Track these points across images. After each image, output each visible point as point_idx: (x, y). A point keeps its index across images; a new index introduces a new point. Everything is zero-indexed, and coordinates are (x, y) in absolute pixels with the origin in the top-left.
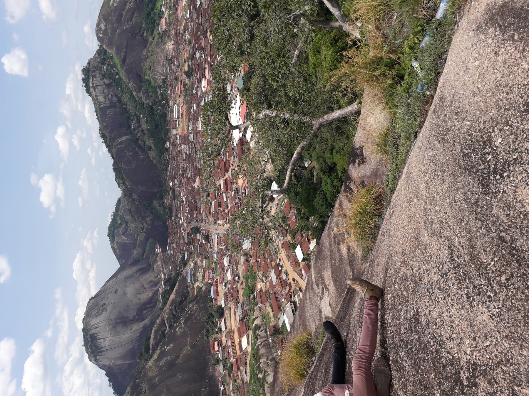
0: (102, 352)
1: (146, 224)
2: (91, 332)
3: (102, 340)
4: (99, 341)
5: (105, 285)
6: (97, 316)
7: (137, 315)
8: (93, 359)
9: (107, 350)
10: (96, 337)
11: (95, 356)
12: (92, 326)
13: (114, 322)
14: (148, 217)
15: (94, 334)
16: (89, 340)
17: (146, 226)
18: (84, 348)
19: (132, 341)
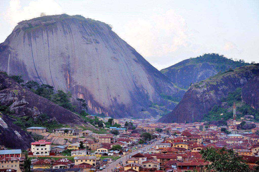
0: (29, 37)
1: (204, 92)
2: (59, 27)
3: (45, 38)
4: (45, 35)
5: (128, 46)
6: (81, 32)
7: (77, 87)
8: (21, 27)
9: (30, 45)
10: (52, 30)
11: (24, 28)
12: (68, 26)
13: (70, 55)
14: (216, 93)
15: (56, 29)
16: (48, 22)
17: (201, 91)
18: (39, 16)
19: (39, 77)
